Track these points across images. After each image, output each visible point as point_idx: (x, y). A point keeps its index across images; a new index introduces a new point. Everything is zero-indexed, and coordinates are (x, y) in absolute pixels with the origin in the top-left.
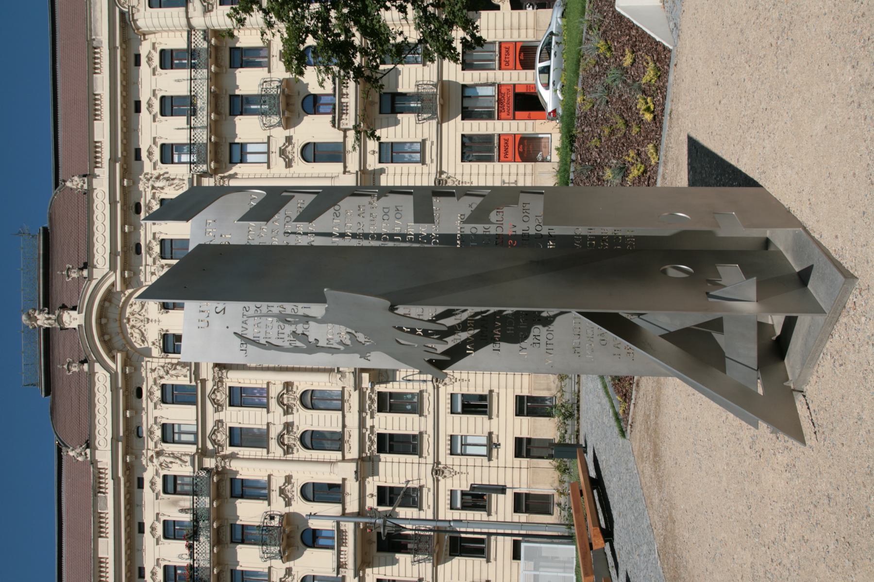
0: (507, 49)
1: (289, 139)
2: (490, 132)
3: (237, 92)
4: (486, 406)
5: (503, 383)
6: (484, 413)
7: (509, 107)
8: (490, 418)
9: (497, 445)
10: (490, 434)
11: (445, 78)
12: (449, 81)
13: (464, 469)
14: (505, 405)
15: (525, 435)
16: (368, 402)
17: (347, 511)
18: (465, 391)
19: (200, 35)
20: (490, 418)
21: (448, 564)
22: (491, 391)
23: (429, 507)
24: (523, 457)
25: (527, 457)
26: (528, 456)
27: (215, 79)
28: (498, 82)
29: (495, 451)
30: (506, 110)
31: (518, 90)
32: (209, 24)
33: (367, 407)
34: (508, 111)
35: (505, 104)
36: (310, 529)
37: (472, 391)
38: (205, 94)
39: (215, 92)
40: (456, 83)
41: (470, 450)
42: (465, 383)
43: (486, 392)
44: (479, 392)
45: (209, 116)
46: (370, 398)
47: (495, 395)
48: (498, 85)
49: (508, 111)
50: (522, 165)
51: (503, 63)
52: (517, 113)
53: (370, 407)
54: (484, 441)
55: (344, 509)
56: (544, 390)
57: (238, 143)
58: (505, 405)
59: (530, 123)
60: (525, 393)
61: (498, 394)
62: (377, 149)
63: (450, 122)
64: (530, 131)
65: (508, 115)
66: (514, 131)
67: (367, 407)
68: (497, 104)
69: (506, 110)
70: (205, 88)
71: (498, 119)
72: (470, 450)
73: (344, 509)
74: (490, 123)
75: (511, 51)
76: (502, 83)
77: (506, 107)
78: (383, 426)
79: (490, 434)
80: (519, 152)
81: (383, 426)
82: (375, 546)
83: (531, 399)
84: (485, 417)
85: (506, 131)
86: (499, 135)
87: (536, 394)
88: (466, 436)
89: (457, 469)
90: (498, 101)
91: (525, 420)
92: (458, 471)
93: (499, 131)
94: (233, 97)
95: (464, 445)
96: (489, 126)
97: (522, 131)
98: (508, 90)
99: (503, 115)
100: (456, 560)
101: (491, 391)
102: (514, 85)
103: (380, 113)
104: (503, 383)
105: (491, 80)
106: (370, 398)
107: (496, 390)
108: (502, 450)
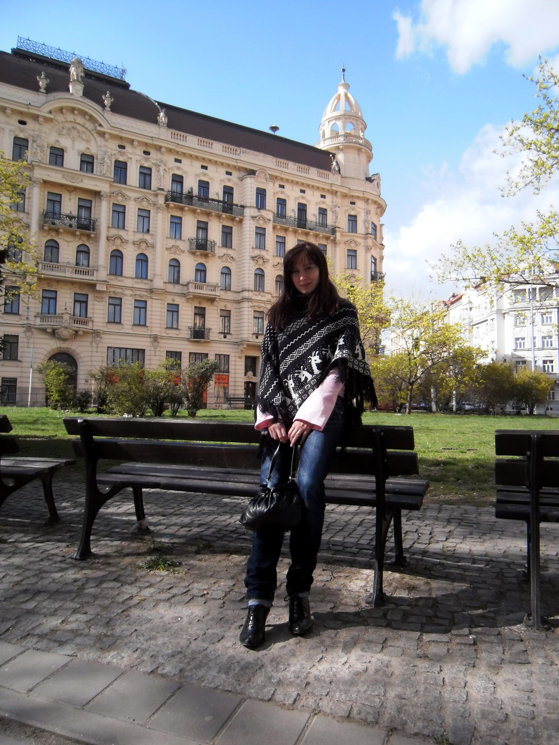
1: (183, 252)
62: (175, 303)
103: (196, 307)
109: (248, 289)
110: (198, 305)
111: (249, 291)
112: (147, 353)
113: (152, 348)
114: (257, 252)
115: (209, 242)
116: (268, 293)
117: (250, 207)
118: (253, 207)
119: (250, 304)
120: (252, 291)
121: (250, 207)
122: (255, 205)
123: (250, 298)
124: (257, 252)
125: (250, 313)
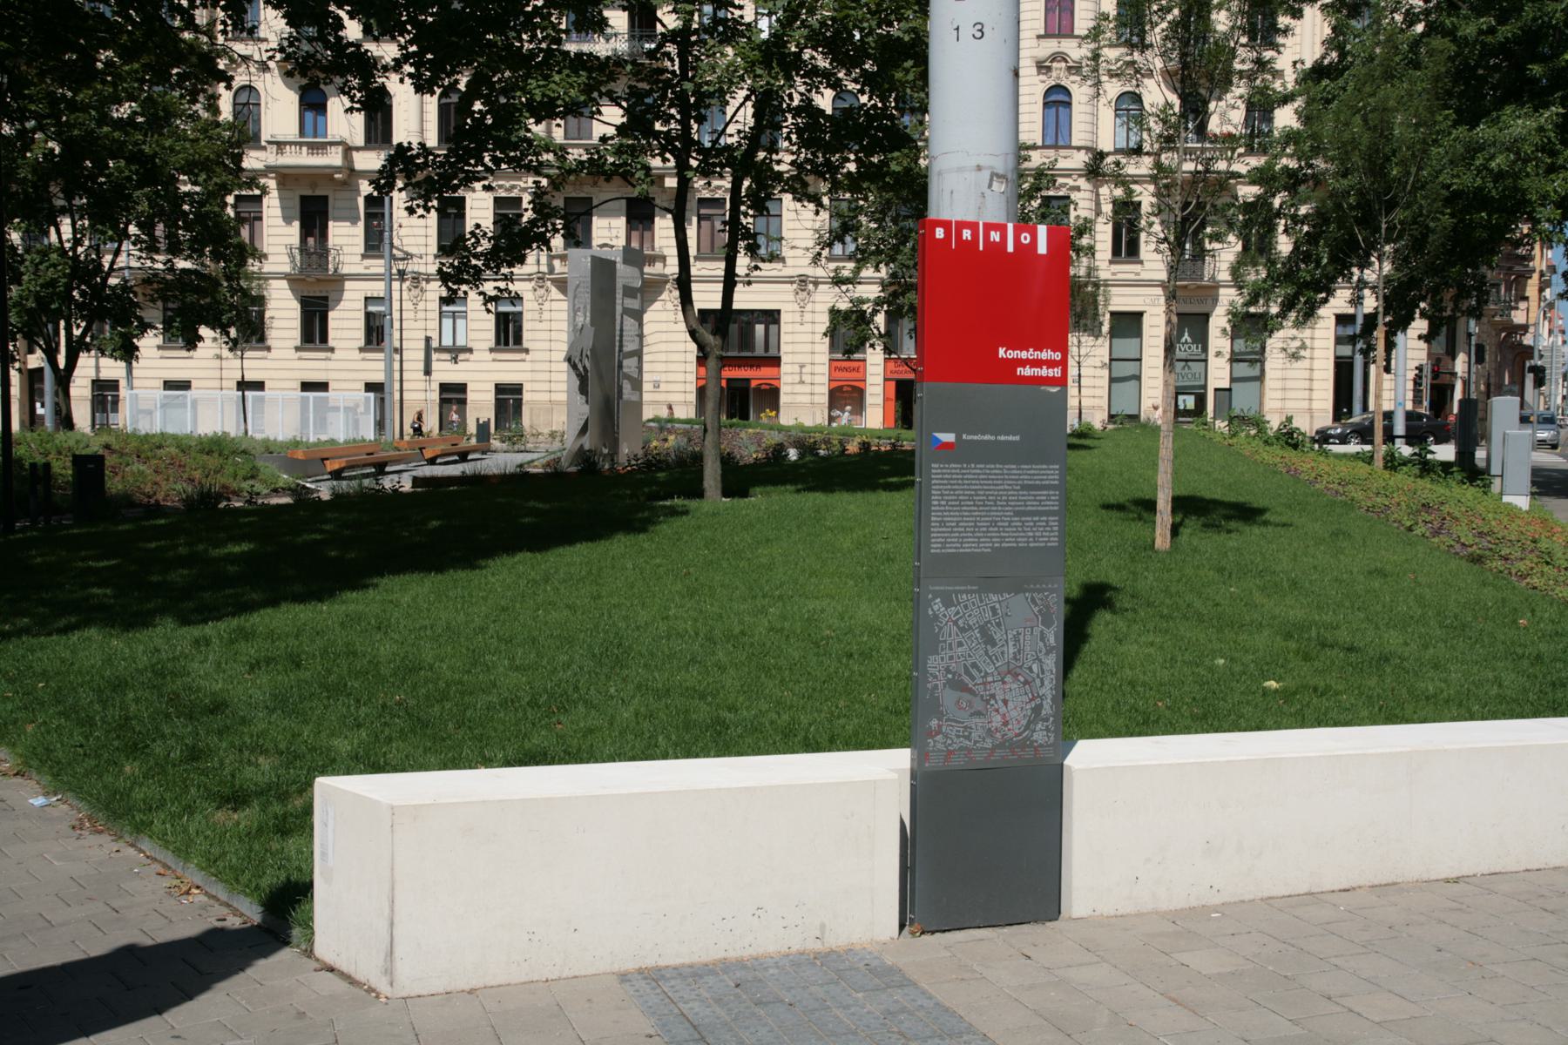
4: (507, 343)
5: (538, 366)
6: (498, 342)
8: (491, 350)
9: (455, 360)
10: (470, 350)
13: (421, 315)
14: (509, 369)
15: (471, 396)
16: (508, 185)
17: (355, 154)
18: (526, 316)
20: (491, 350)
21: (289, 294)
22: (527, 351)
23: (367, 268)
24: (441, 394)
25: (441, 399)
26: (443, 401)
29: (447, 356)
33: (500, 183)
36: (326, 100)
37: (526, 326)
41: (448, 323)
42: (537, 316)
43: (525, 344)
44: (526, 335)
46: (513, 187)
47: (523, 356)
50: (825, 390)
52: (893, 383)
53: (501, 187)
54: (461, 342)
55: (358, 149)
56: (531, 419)
58: (509, 369)
59: (880, 400)
60: (526, 396)
61: (524, 361)
64: (869, 400)
66: (869, 380)
67: (500, 183)
72: (448, 323)
73: (358, 149)
78: (476, 204)
79: (470, 350)
80: (842, 387)
81: (476, 204)
82: (308, 193)
83: (519, 404)
84: (492, 344)
85: (870, 369)
86: (864, 360)
87: (525, 410)
88: (466, 317)
89: (421, 306)
91: (490, 397)
92: (419, 307)
95: (454, 315)
97: (869, 390)
99: (891, 365)
100: (296, 305)
101: (527, 351)
104: (538, 366)
106: (513, 187)
107: (528, 357)
108: (449, 366)
112: (784, 318)
113: (796, 307)
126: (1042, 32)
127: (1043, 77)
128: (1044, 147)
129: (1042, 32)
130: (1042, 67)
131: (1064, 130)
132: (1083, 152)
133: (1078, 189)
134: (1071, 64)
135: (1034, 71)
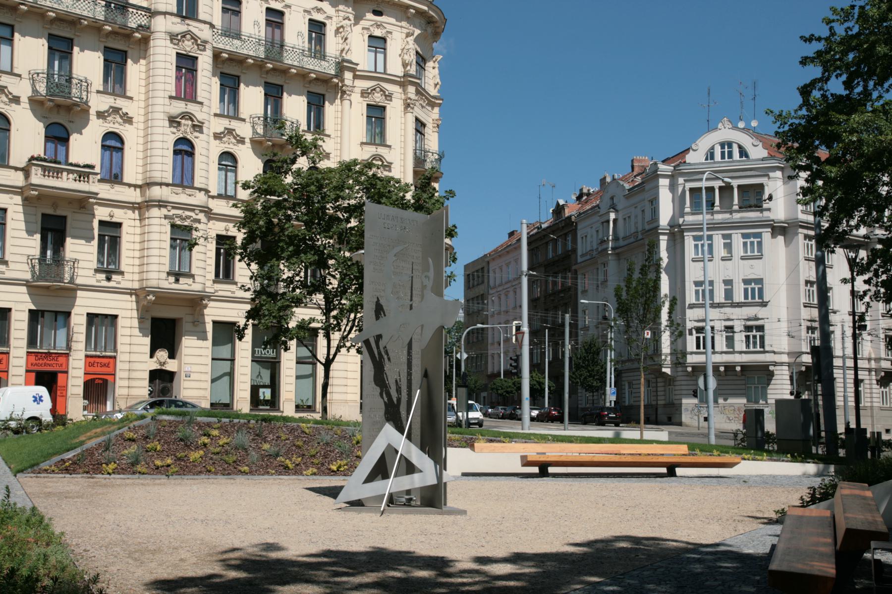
0: (108, 365)
2: (13, 342)
3: (76, 49)
7: (41, 365)
11: (80, 293)
12: (75, 297)
19: (144, 21)
27: (95, 27)
28: (71, 353)
30: (37, 362)
31: (60, 375)
32: (157, 35)
34: (36, 364)
35: (45, 361)
38: (78, 12)
39: (81, 23)
40: (73, 306)
45: (53, 10)
48: (68, 354)
49: (36, 364)
51: (92, 360)
52: (34, 374)
57: (13, 35)
63: (27, 296)
65: (32, 364)
68: (46, 351)
69: (37, 362)
70: (85, 13)
71: (28, 352)
74: (24, 343)
75: (105, 370)
76: (71, 358)
77: (41, 362)
85: (13, 361)
86: (8, 353)
90: (49, 353)
93: (13, 353)
94: (70, 43)
96: (20, 341)
98: (62, 365)
99: (32, 358)
102: (67, 372)
103: (44, 215)
105: (74, 346)
109: (159, 180)
110: (50, 211)
111: (161, 184)
114: (179, 107)
115: (74, 81)
116: (200, 190)
117: (165, 13)
118: (171, 14)
119: (164, 211)
120: (167, 185)
121: (165, 13)
122: (175, 11)
123: (164, 199)
124: (179, 107)
125: (163, 229)
126: (174, 94)
127: (174, 130)
128: (173, 185)
129: (174, 94)
130: (173, 121)
131: (187, 174)
132: (203, 192)
133: (199, 221)
134: (196, 123)
135: (167, 123)
